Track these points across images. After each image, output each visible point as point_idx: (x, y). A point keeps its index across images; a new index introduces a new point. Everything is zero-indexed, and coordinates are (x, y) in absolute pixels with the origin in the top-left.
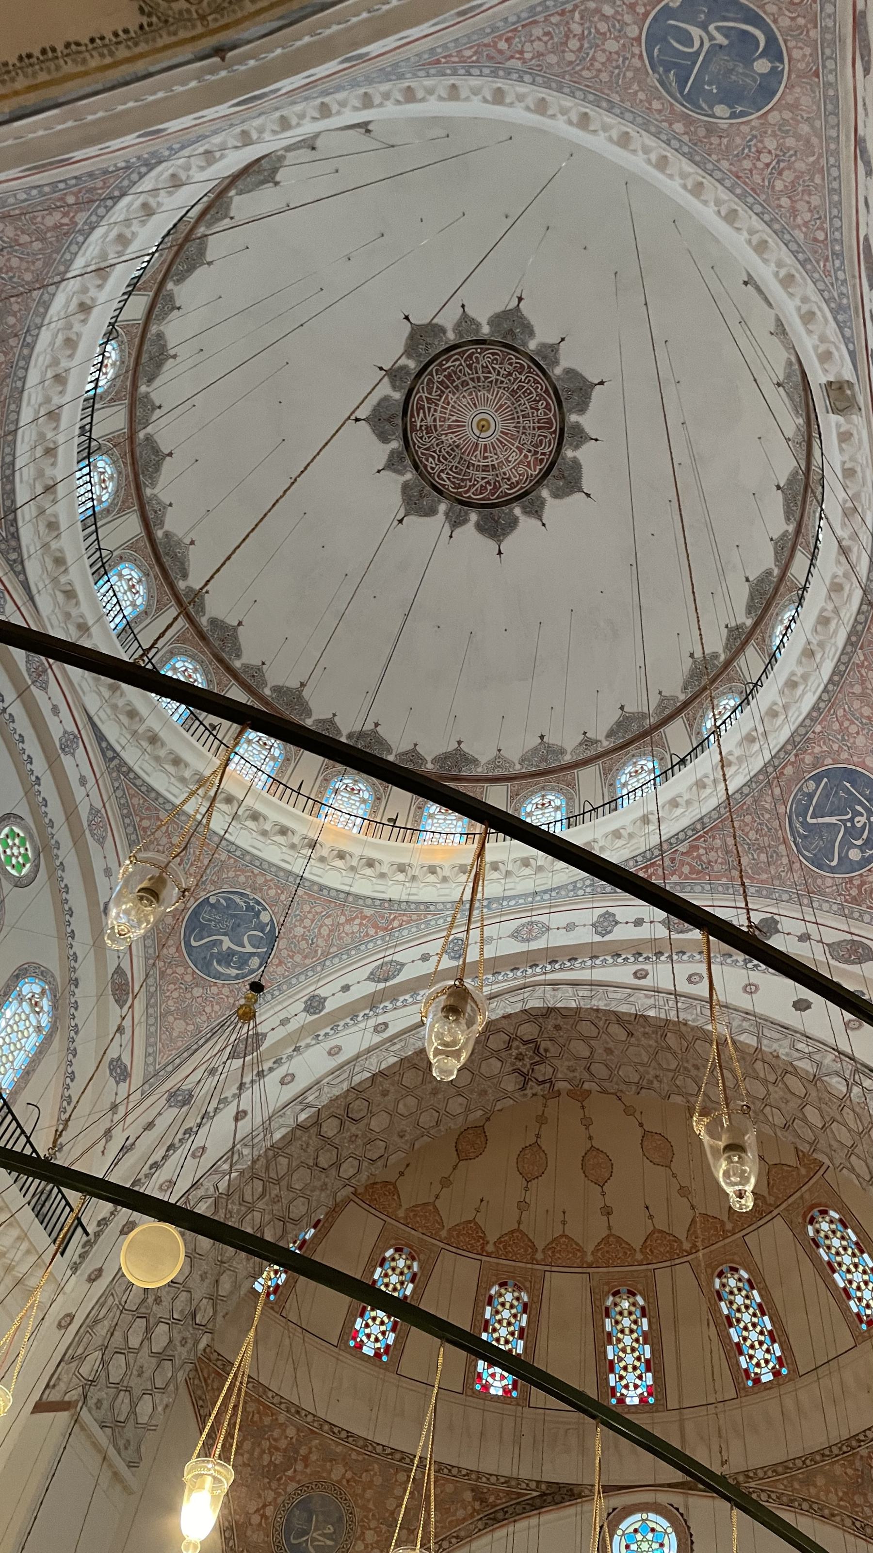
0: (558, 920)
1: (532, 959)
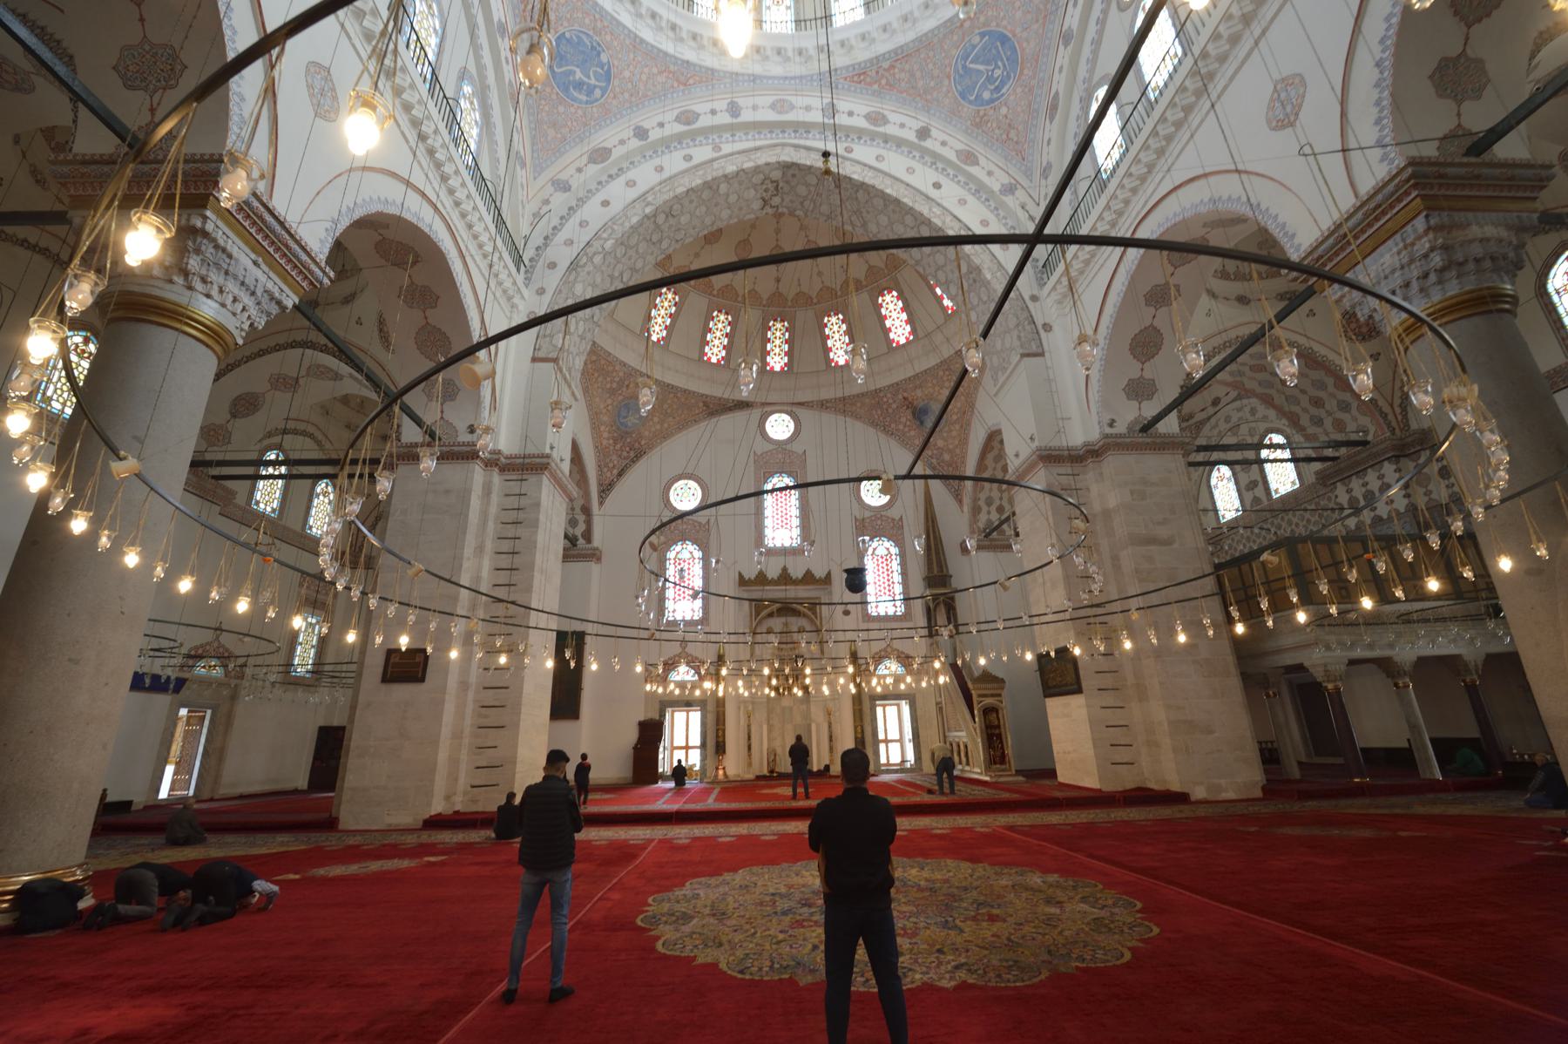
0: (799, 101)
1: (783, 126)
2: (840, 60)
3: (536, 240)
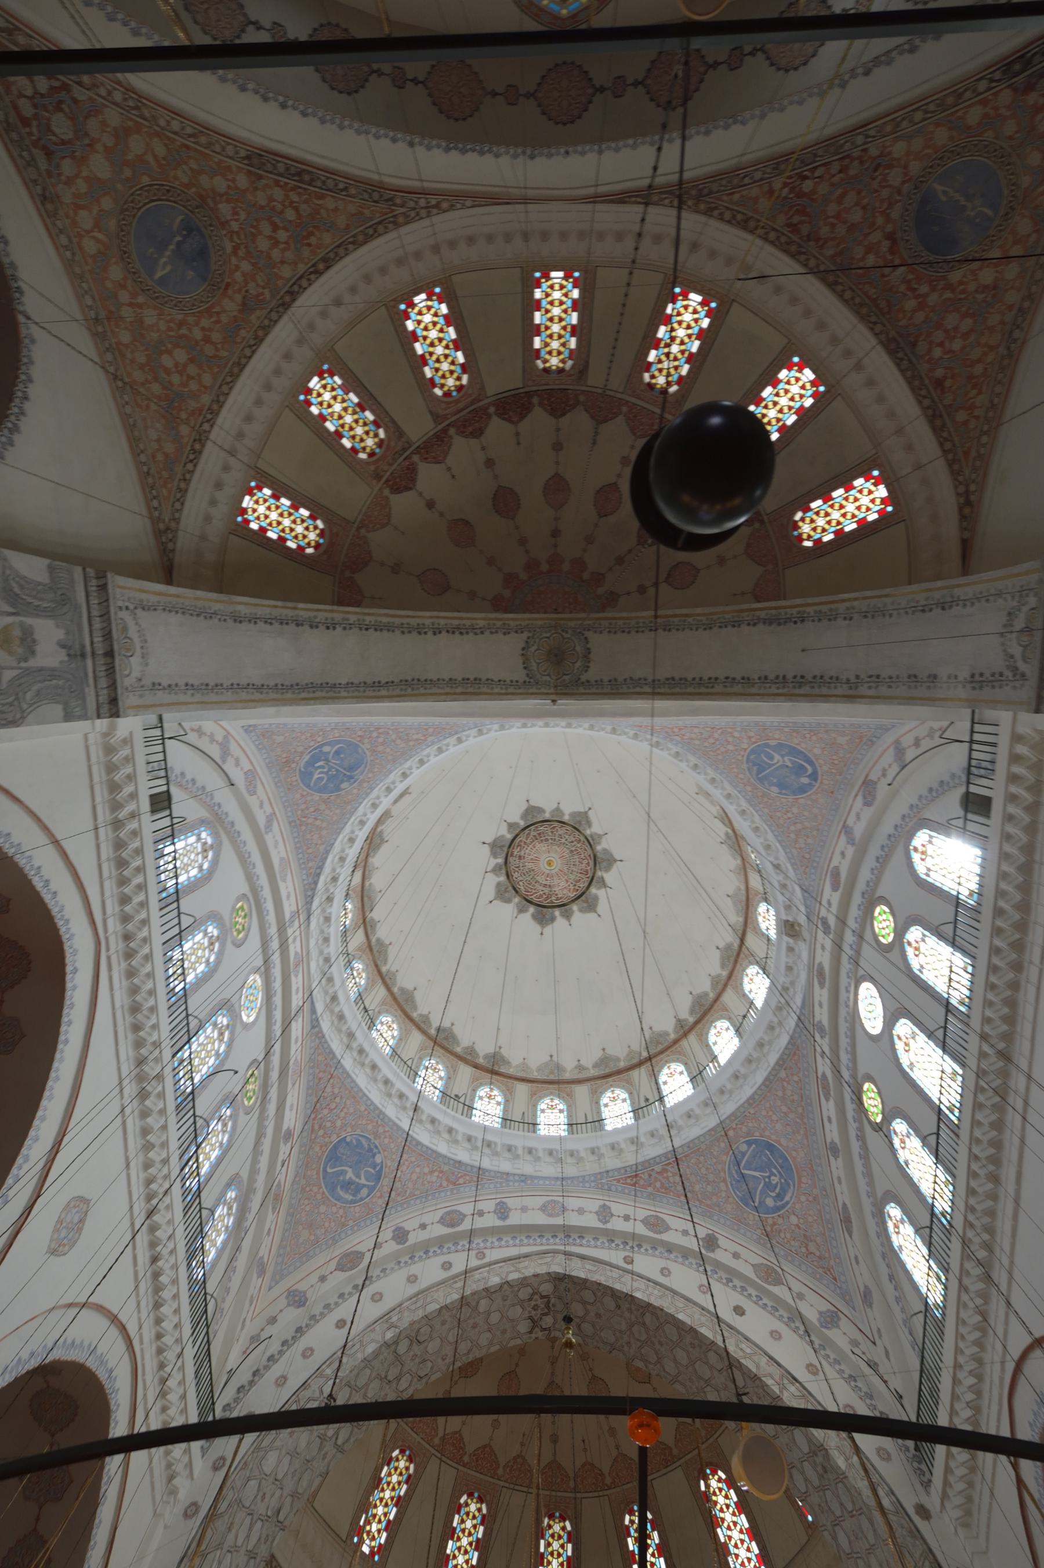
2: (611, 1162)
3: (243, 1377)
